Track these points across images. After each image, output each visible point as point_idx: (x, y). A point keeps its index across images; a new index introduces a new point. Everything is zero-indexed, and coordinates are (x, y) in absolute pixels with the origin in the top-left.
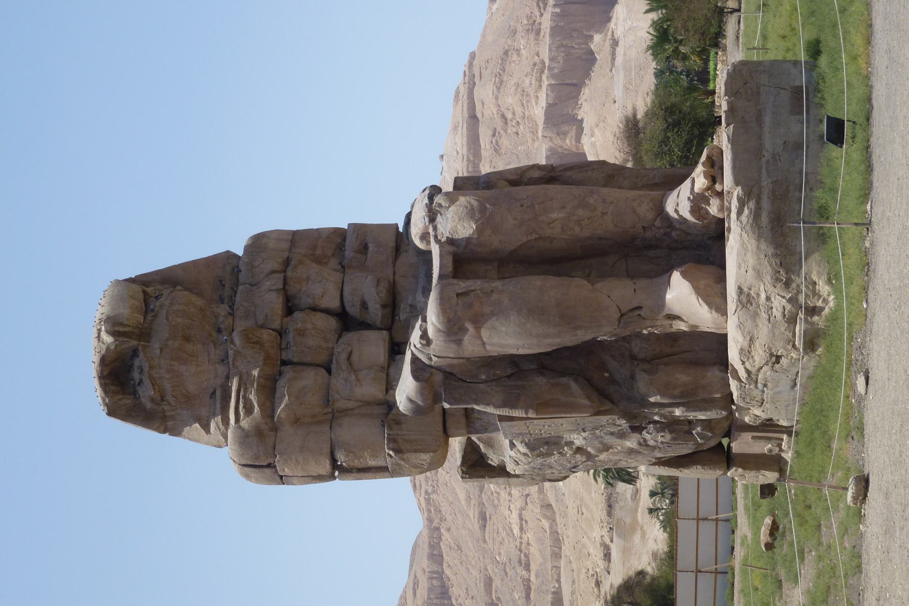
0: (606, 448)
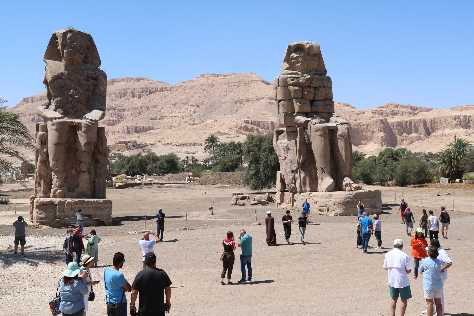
0: (287, 164)
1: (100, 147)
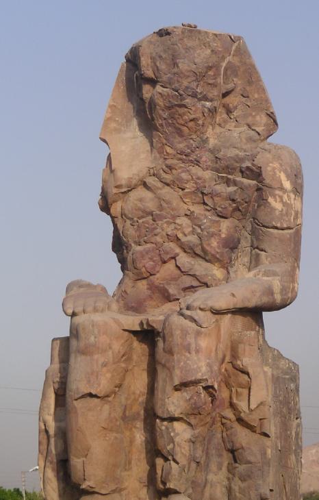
1: (242, 405)
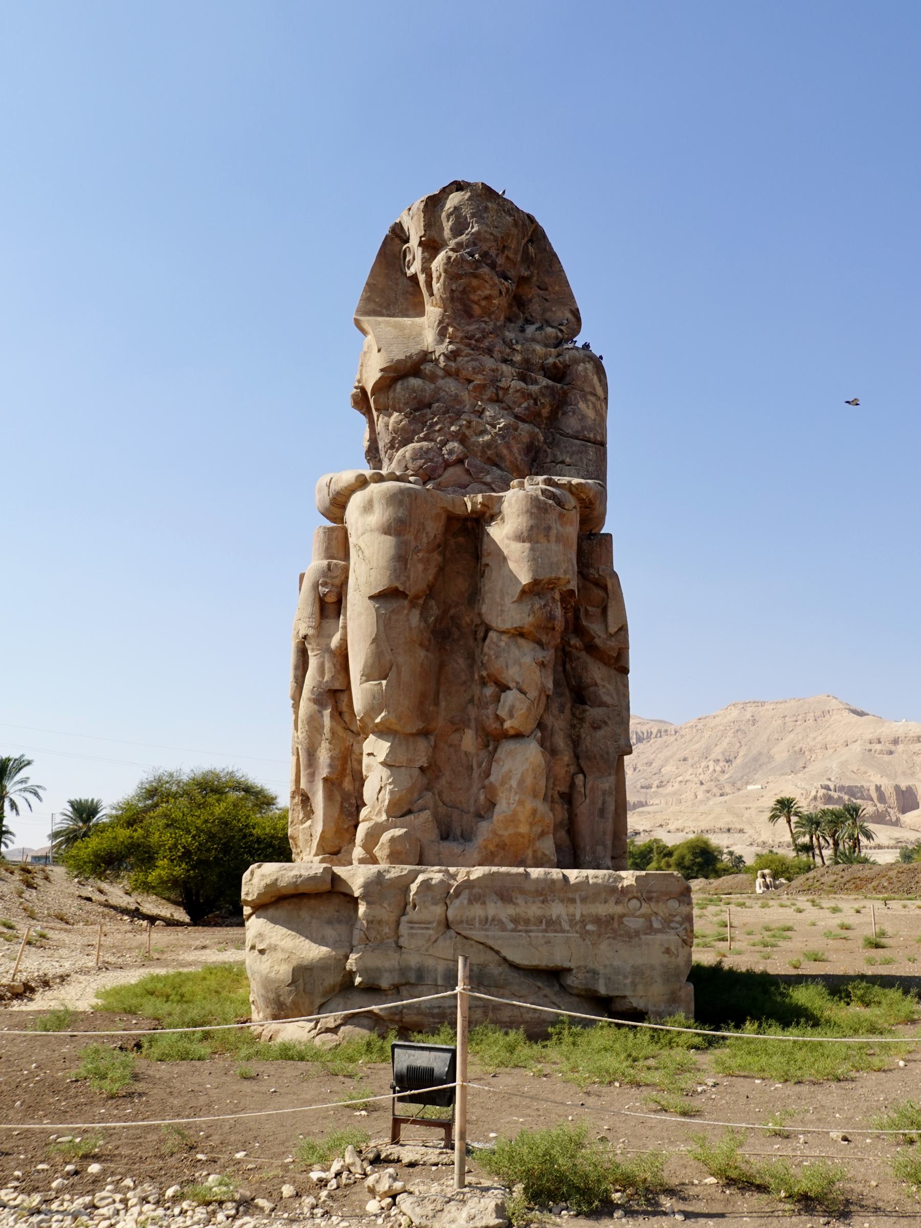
1: (595, 628)
